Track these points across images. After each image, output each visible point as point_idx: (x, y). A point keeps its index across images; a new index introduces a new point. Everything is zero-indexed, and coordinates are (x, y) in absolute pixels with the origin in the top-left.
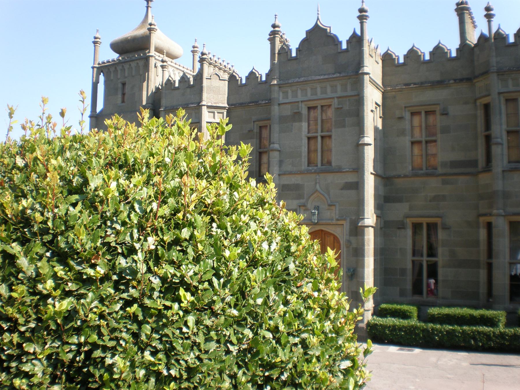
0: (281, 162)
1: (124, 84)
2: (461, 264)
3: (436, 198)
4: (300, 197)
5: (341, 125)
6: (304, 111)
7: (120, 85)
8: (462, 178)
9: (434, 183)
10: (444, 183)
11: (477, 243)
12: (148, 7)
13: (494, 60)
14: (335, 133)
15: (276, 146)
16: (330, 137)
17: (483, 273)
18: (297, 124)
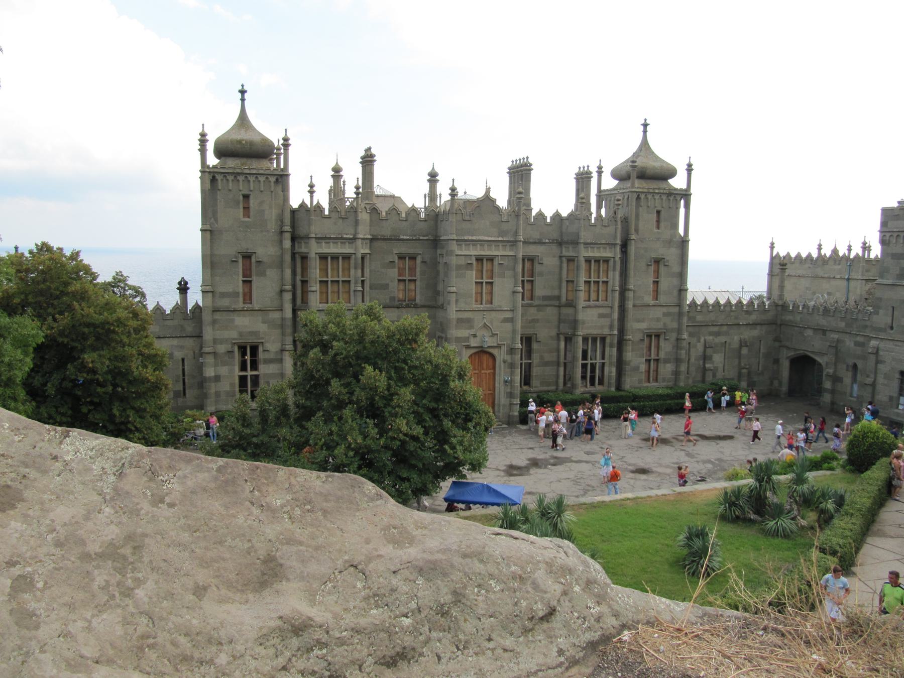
0: (457, 301)
1: (246, 197)
2: (546, 364)
3: (534, 321)
4: (471, 327)
5: (502, 276)
6: (474, 262)
7: (241, 197)
8: (549, 309)
9: (532, 310)
10: (538, 310)
11: (558, 350)
12: (243, 100)
13: (582, 234)
14: (496, 281)
15: (454, 289)
16: (491, 283)
17: (562, 369)
18: (469, 272)
